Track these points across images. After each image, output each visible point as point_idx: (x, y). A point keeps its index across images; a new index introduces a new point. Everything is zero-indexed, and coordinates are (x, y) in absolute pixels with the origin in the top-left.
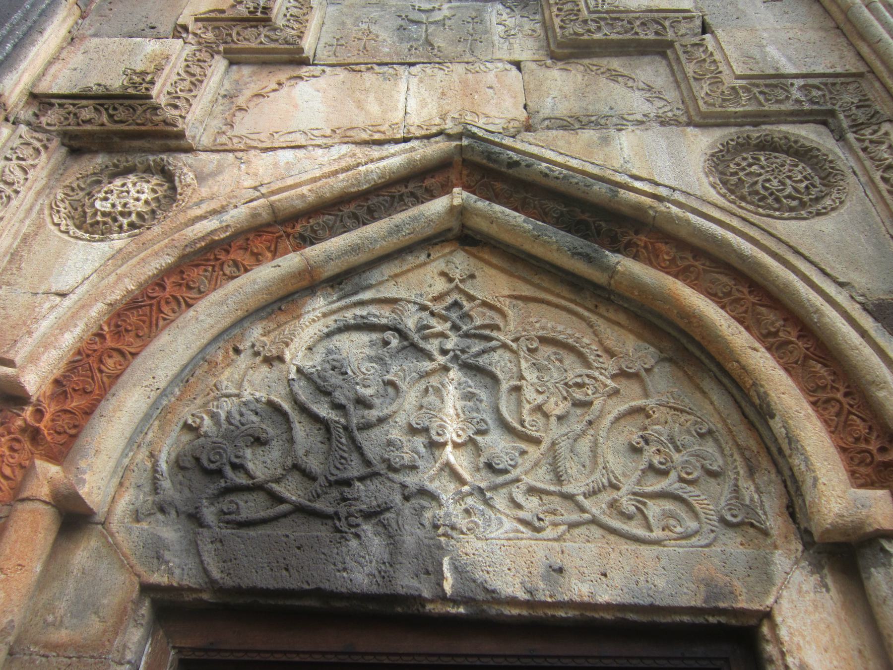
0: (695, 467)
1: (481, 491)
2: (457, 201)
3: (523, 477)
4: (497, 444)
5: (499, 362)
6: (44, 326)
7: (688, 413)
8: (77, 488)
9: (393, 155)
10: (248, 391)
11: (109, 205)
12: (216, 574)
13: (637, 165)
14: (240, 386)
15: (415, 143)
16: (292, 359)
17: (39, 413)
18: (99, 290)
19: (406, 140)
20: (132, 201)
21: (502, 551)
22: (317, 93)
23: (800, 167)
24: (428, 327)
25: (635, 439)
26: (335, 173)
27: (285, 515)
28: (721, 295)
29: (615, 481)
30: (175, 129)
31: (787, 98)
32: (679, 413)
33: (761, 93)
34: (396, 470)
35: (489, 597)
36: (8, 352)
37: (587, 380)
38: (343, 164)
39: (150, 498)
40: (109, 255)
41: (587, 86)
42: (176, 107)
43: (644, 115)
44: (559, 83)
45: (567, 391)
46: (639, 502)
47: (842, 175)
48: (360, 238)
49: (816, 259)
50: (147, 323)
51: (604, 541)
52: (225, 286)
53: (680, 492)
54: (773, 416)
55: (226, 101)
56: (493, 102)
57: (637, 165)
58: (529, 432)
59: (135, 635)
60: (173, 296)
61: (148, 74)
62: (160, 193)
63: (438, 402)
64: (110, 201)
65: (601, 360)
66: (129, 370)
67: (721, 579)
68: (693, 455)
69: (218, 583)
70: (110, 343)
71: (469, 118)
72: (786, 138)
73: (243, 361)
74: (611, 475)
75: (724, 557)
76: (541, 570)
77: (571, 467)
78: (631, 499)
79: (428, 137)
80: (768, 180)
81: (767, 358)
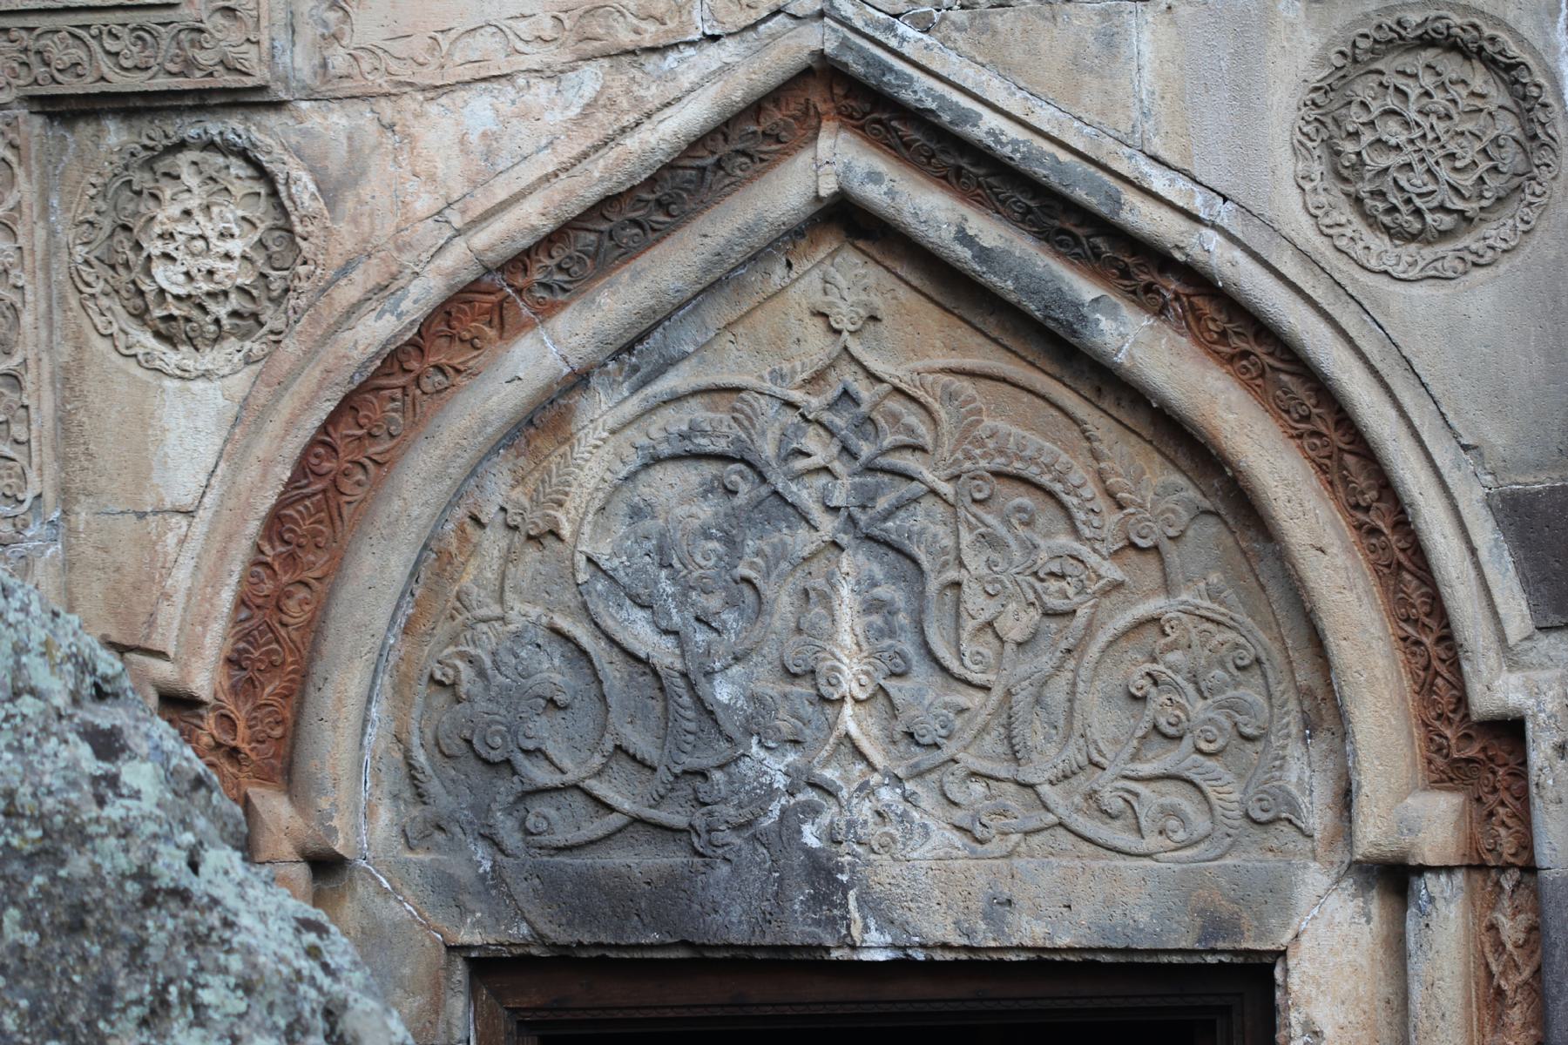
1: (900, 780)
4: (920, 692)
6: (181, 578)
11: (182, 278)
13: (1165, 127)
14: (501, 600)
15: (728, 51)
16: (577, 534)
17: (227, 721)
18: (243, 498)
21: (928, 880)
25: (1139, 682)
28: (1296, 416)
29: (1096, 758)
36: (148, 637)
37: (1069, 570)
38: (597, 135)
39: (416, 811)
45: (1035, 591)
46: (1129, 791)
48: (653, 294)
50: (327, 521)
57: (1165, 127)
59: (458, 1005)
62: (262, 227)
63: (826, 624)
67: (1226, 908)
68: (1221, 707)
73: (493, 542)
77: (1034, 734)
78: (1117, 789)
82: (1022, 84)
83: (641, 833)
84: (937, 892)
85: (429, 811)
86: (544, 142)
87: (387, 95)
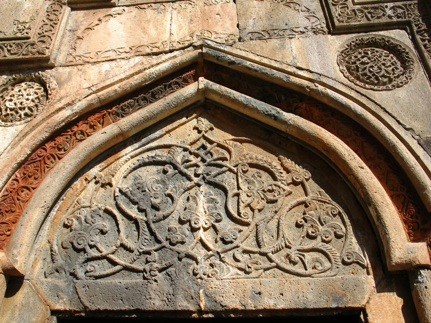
0: (330, 234)
1: (218, 253)
2: (201, 86)
3: (240, 245)
4: (227, 226)
5: (228, 180)
7: (328, 203)
8: (14, 265)
9: (164, 61)
10: (95, 203)
11: (13, 104)
12: (87, 304)
13: (300, 61)
15: (175, 53)
19: (171, 51)
20: (25, 101)
22: (120, 25)
23: (390, 57)
24: (188, 161)
26: (132, 75)
27: (118, 271)
29: (288, 244)
30: (44, 56)
31: (384, 15)
32: (323, 204)
33: (369, 13)
34: (173, 245)
35: (223, 309)
37: (274, 188)
38: (137, 69)
40: (16, 135)
41: (272, 10)
42: (43, 42)
43: (305, 28)
44: (257, 9)
45: (264, 195)
46: (300, 254)
47: (412, 61)
49: (395, 115)
50: (40, 170)
51: (282, 276)
52: (78, 146)
53: (322, 248)
54: (370, 205)
55: (71, 34)
56: (219, 23)
58: (243, 220)
60: (50, 154)
61: (27, 23)
63: (195, 205)
64: (13, 102)
65: (282, 175)
66: (33, 198)
69: (88, 308)
70: (22, 184)
71: (206, 35)
72: (383, 39)
74: (286, 241)
75: (343, 281)
76: (249, 294)
77: (265, 237)
79: (183, 48)
80: (372, 67)
81: (368, 173)
82: (259, 54)
83: (126, 273)
84: (233, 290)
85: (54, 265)
86: (122, 72)
87: (81, 65)
